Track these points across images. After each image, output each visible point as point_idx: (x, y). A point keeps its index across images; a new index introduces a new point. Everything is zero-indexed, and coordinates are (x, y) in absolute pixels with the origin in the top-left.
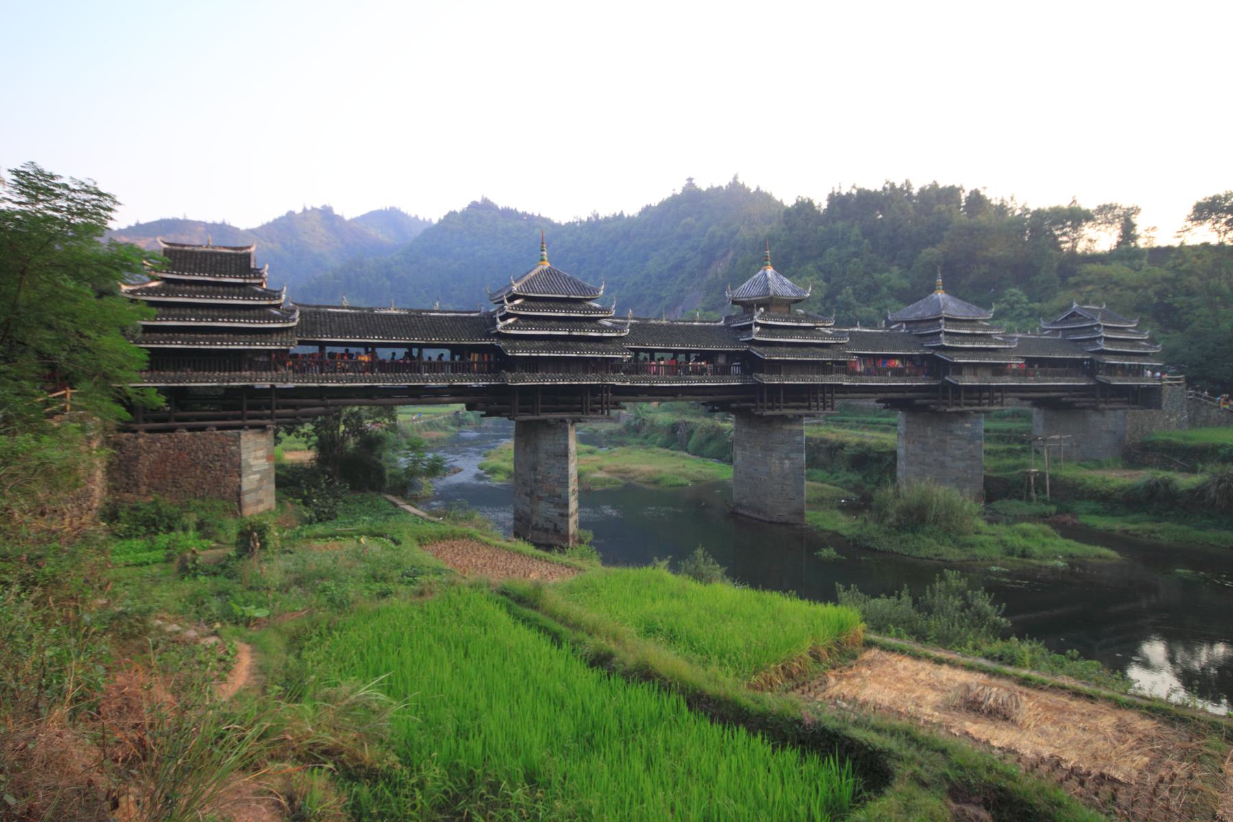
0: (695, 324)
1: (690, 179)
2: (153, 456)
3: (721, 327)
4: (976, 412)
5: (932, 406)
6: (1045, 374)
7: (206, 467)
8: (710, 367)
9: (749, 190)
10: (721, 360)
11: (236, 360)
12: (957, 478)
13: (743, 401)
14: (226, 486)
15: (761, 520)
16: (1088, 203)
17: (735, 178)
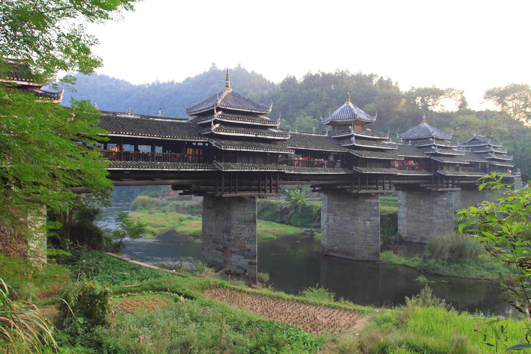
0: (313, 135)
1: (214, 64)
3: (326, 137)
4: (451, 191)
5: (428, 188)
6: (469, 171)
8: (326, 162)
9: (248, 72)
10: (331, 159)
12: (440, 229)
13: (343, 184)
15: (349, 259)
17: (239, 65)
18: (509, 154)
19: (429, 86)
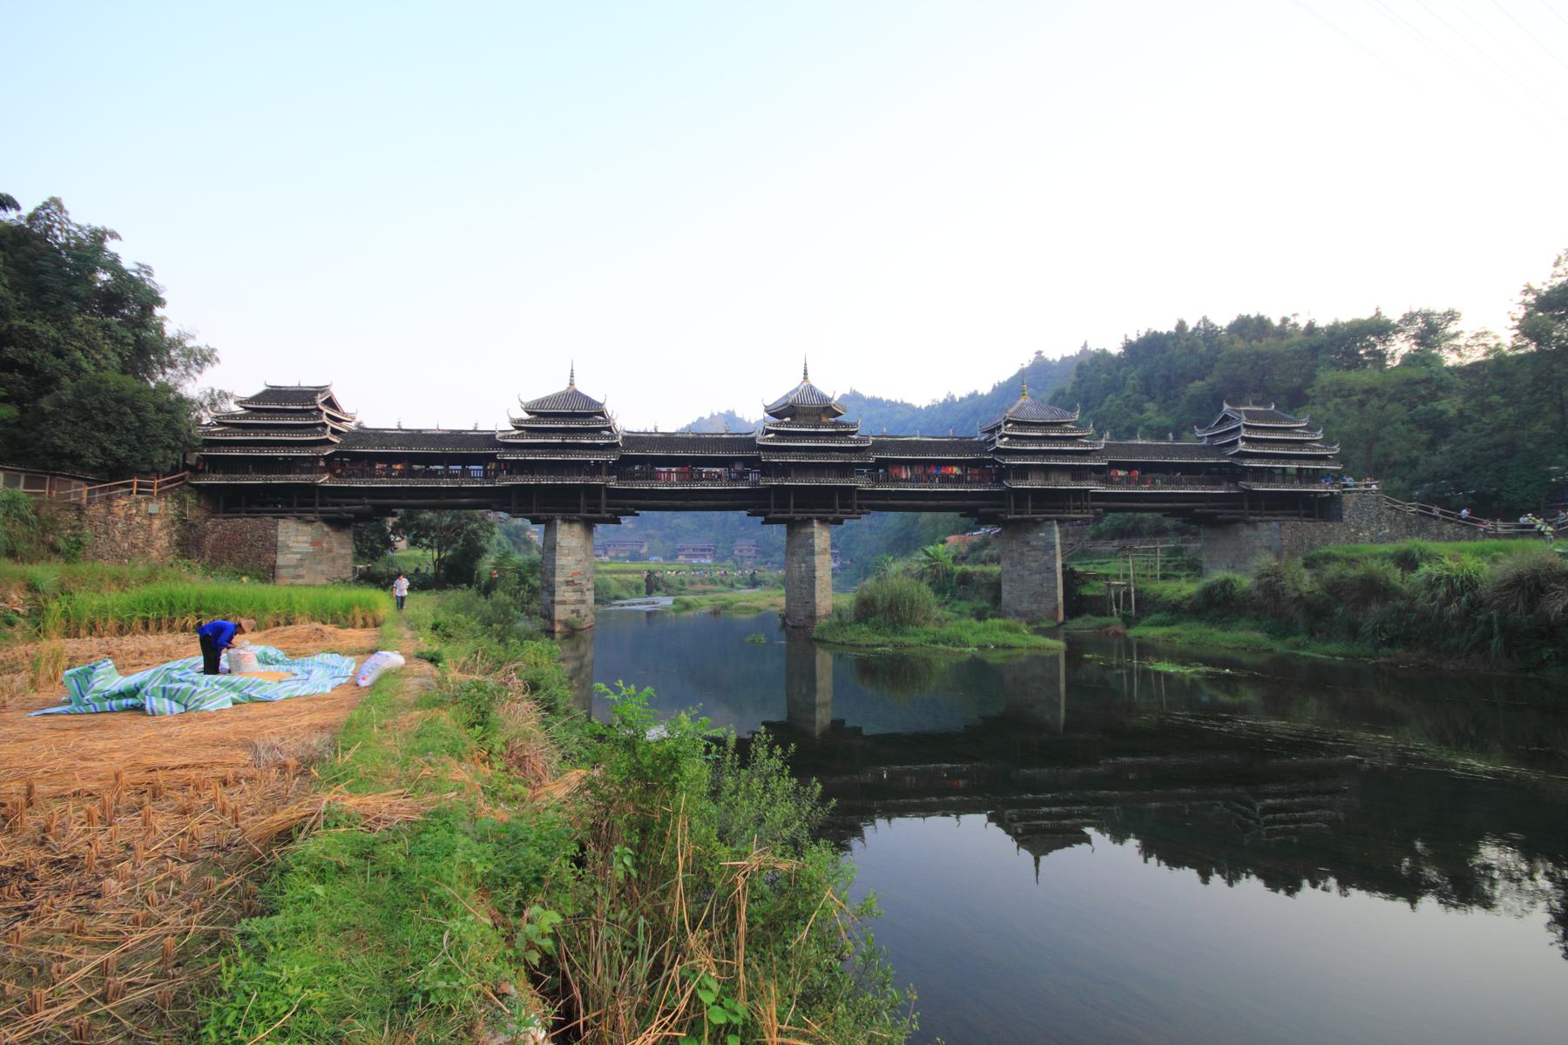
1: (1039, 353)
2: (214, 536)
5: (1001, 515)
7: (252, 545)
11: (289, 465)
14: (266, 561)
16: (1394, 315)
18: (1327, 441)
19: (1365, 314)
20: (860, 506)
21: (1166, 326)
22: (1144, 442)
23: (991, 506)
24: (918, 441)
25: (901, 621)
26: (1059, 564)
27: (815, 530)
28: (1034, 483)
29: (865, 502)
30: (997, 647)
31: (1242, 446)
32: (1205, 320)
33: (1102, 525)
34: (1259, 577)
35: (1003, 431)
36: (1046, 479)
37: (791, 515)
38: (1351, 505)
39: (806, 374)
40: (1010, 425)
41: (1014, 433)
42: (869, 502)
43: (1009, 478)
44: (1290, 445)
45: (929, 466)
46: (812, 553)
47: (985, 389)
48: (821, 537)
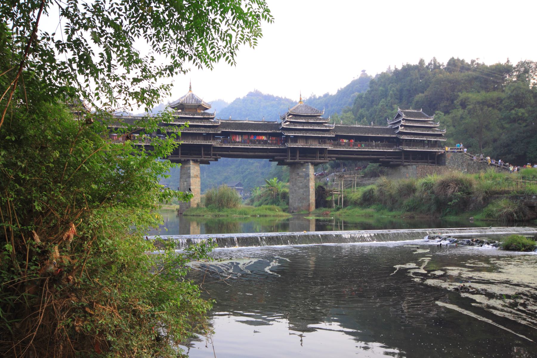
1: (364, 71)
18: (441, 128)
20: (214, 155)
21: (415, 62)
22: (359, 126)
23: (281, 156)
24: (247, 123)
25: (223, 206)
26: (312, 185)
27: (191, 166)
28: (300, 145)
29: (218, 152)
30: (260, 216)
31: (401, 129)
32: (435, 60)
33: (366, 170)
34: (378, 186)
35: (286, 119)
36: (306, 143)
37: (180, 158)
38: (450, 158)
39: (190, 88)
40: (290, 116)
41: (292, 120)
42: (221, 153)
43: (288, 142)
44: (425, 129)
45: (251, 136)
46: (189, 177)
47: (333, 92)
48: (194, 169)
